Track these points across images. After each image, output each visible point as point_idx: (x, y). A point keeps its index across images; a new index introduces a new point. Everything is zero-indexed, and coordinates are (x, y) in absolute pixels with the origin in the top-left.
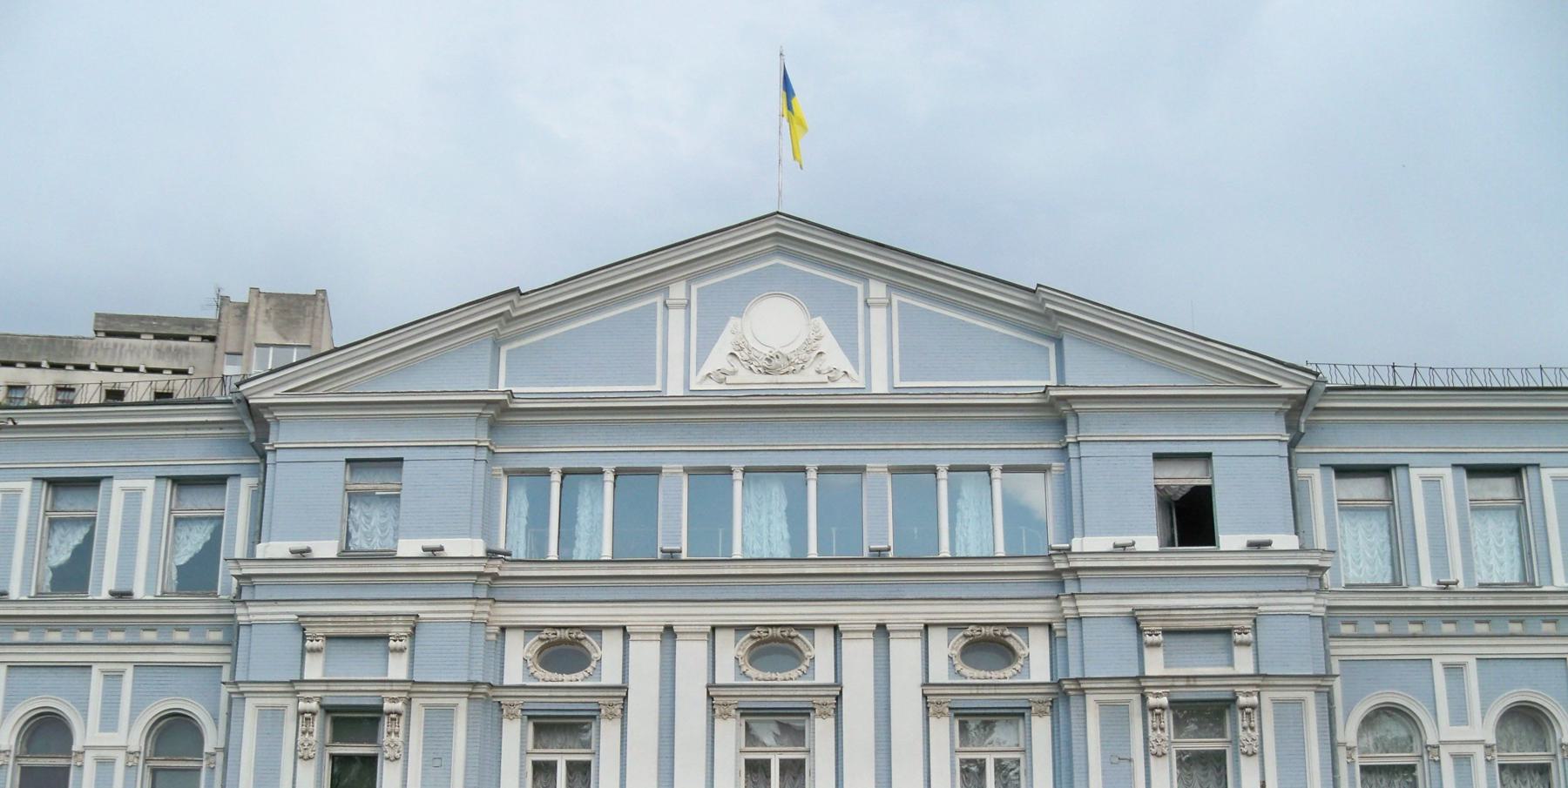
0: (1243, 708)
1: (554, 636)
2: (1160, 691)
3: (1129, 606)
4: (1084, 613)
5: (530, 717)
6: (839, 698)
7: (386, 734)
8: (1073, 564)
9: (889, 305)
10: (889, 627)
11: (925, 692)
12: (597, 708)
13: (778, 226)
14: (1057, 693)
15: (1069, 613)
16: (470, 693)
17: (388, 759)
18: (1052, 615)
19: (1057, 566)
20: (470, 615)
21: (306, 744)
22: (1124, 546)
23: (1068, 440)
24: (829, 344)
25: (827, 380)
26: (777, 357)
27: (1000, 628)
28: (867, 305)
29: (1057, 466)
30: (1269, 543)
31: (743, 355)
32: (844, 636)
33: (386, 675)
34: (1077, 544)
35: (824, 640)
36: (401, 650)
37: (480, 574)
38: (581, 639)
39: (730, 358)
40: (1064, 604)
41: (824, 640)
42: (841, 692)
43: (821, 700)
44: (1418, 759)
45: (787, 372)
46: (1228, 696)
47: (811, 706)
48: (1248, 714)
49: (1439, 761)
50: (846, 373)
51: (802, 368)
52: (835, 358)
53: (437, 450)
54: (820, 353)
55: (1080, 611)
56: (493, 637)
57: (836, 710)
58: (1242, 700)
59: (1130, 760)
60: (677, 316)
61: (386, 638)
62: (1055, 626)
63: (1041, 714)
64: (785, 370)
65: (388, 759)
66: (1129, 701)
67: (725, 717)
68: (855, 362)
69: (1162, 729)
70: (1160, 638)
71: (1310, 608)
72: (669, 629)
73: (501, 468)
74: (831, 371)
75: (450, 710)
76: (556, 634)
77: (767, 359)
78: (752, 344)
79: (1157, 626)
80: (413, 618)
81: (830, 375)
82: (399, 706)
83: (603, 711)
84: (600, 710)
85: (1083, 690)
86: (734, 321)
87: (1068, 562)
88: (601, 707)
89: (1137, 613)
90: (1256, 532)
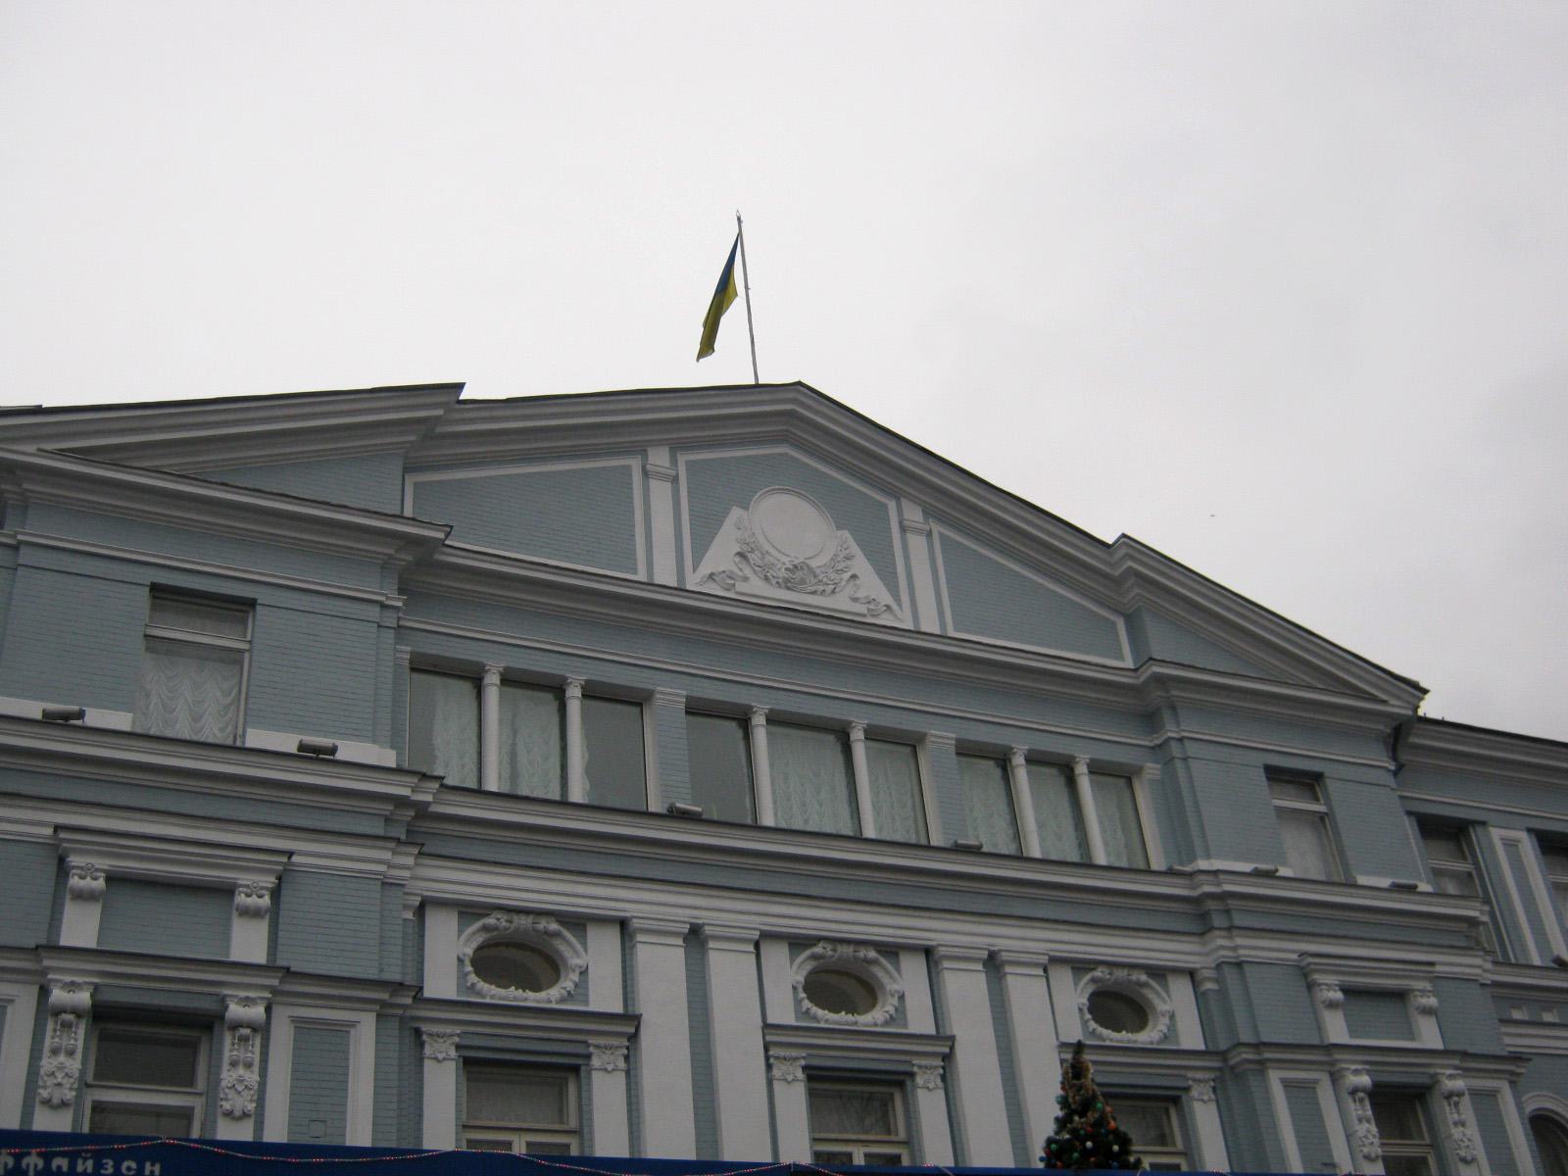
0: (1449, 1096)
1: (508, 925)
3: (1293, 951)
4: (1245, 956)
7: (225, 1066)
8: (1228, 888)
9: (929, 534)
13: (794, 401)
14: (1220, 1069)
16: (384, 1004)
20: (382, 868)
23: (1170, 734)
24: (861, 565)
25: (866, 612)
26: (802, 568)
28: (903, 529)
29: (1152, 769)
35: (913, 970)
36: (255, 913)
37: (400, 802)
39: (737, 559)
41: (913, 970)
45: (814, 593)
50: (888, 607)
51: (833, 592)
52: (871, 585)
53: (315, 598)
54: (854, 577)
56: (409, 915)
57: (944, 1078)
61: (227, 891)
64: (813, 589)
66: (1316, 1082)
70: (1339, 995)
71: (1478, 971)
73: (409, 649)
74: (869, 602)
75: (342, 1031)
77: (787, 569)
78: (767, 547)
80: (284, 859)
81: (872, 607)
82: (257, 1012)
84: (588, 1056)
85: (1261, 1062)
86: (736, 513)
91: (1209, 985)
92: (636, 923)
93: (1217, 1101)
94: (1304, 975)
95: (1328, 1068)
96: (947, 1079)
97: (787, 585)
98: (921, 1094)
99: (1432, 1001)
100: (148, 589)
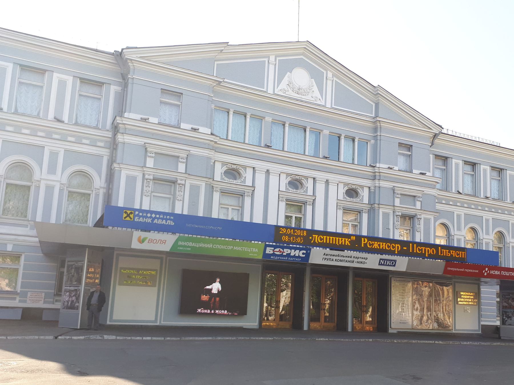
0: (418, 219)
2: (399, 211)
3: (392, 186)
5: (221, 192)
6: (314, 200)
8: (380, 171)
10: (330, 181)
11: (337, 202)
12: (243, 192)
14: (370, 208)
15: (377, 185)
17: (178, 200)
18: (372, 185)
19: (376, 171)
21: (148, 191)
27: (357, 186)
30: (425, 174)
32: (317, 181)
33: (178, 171)
34: (378, 165)
38: (240, 169)
40: (376, 182)
42: (315, 198)
43: (309, 200)
44: (448, 238)
46: (415, 215)
47: (306, 201)
48: (419, 220)
49: (454, 239)
55: (380, 185)
57: (313, 204)
58: (419, 217)
59: (389, 229)
62: (372, 188)
63: (365, 212)
65: (178, 200)
67: (282, 201)
69: (398, 222)
70: (400, 196)
71: (435, 193)
72: (268, 171)
76: (232, 166)
79: (399, 192)
83: (246, 194)
84: (245, 193)
87: (379, 170)
88: (245, 192)
89: (395, 188)
90: (422, 171)
91: (372, 190)
92: (256, 169)
93: (368, 214)
94: (393, 190)
95: (393, 210)
96: (313, 204)
98: (308, 206)
99: (421, 199)
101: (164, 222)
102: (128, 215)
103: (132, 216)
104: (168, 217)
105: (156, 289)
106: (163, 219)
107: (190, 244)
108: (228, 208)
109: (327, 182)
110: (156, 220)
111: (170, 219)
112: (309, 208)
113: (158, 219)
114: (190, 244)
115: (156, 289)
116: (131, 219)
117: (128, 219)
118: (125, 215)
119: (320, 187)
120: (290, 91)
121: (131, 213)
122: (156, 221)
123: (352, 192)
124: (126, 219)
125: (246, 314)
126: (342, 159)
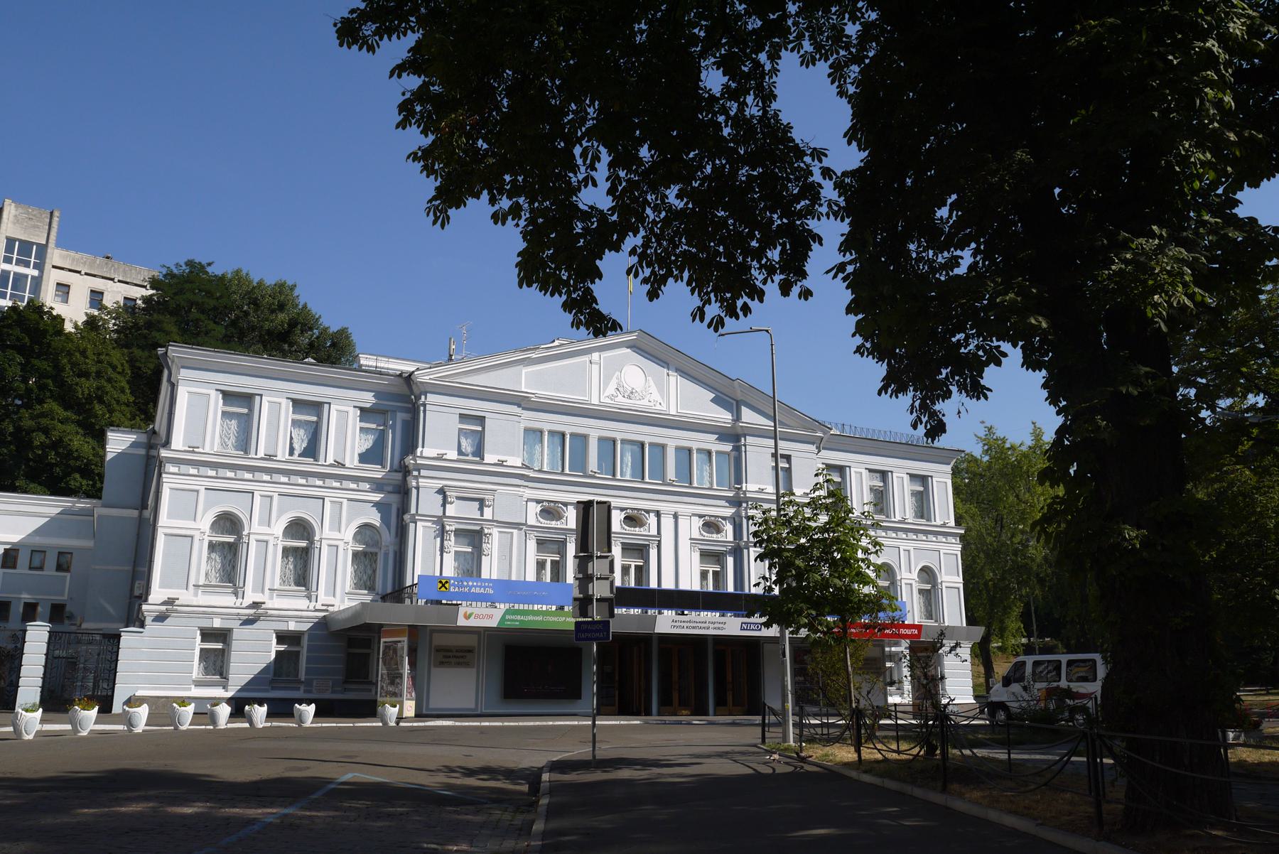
22: (763, 490)
24: (653, 389)
31: (621, 389)
52: (656, 396)
60: (595, 367)
68: (663, 398)
78: (625, 385)
86: (618, 373)
97: (629, 398)
100: (458, 415)
101: (482, 590)
102: (443, 585)
103: (447, 585)
104: (487, 584)
105: (474, 670)
106: (481, 587)
107: (519, 617)
108: (512, 533)
109: (676, 516)
110: (474, 588)
111: (488, 587)
112: (653, 553)
113: (475, 587)
114: (519, 617)
115: (474, 670)
116: (446, 589)
117: (443, 589)
118: (440, 585)
119: (667, 522)
120: (620, 396)
121: (447, 582)
122: (473, 590)
123: (711, 525)
124: (442, 589)
125: (580, 698)
126: (695, 485)
